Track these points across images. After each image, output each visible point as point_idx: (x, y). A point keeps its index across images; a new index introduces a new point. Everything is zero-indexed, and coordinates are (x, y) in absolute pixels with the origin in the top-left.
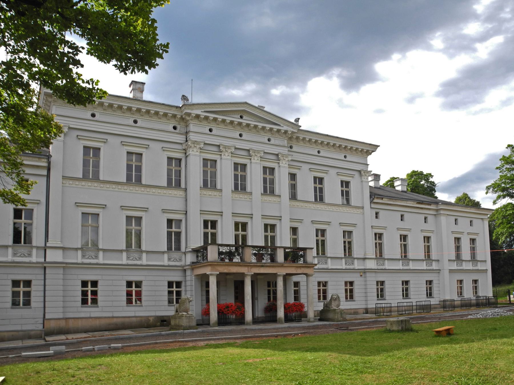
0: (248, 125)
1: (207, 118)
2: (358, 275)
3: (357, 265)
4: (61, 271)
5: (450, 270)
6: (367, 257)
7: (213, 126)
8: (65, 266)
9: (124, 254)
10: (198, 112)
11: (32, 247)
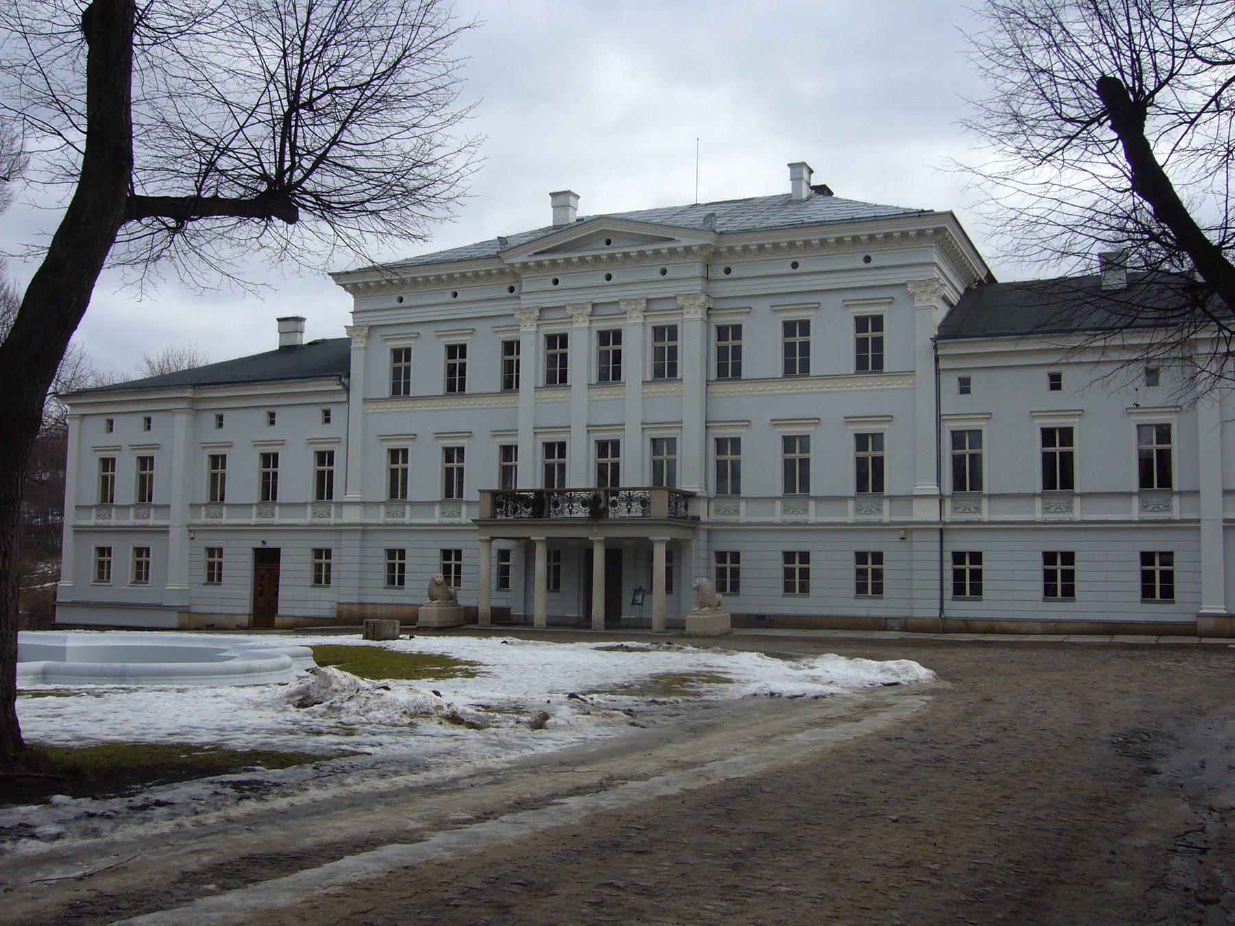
0: (612, 257)
1: (539, 264)
2: (896, 537)
3: (887, 513)
4: (358, 535)
5: (1226, 520)
6: (915, 493)
7: (555, 274)
8: (364, 530)
9: (851, 505)
10: (523, 258)
11: (981, 496)
